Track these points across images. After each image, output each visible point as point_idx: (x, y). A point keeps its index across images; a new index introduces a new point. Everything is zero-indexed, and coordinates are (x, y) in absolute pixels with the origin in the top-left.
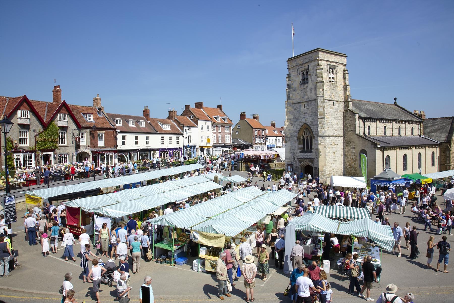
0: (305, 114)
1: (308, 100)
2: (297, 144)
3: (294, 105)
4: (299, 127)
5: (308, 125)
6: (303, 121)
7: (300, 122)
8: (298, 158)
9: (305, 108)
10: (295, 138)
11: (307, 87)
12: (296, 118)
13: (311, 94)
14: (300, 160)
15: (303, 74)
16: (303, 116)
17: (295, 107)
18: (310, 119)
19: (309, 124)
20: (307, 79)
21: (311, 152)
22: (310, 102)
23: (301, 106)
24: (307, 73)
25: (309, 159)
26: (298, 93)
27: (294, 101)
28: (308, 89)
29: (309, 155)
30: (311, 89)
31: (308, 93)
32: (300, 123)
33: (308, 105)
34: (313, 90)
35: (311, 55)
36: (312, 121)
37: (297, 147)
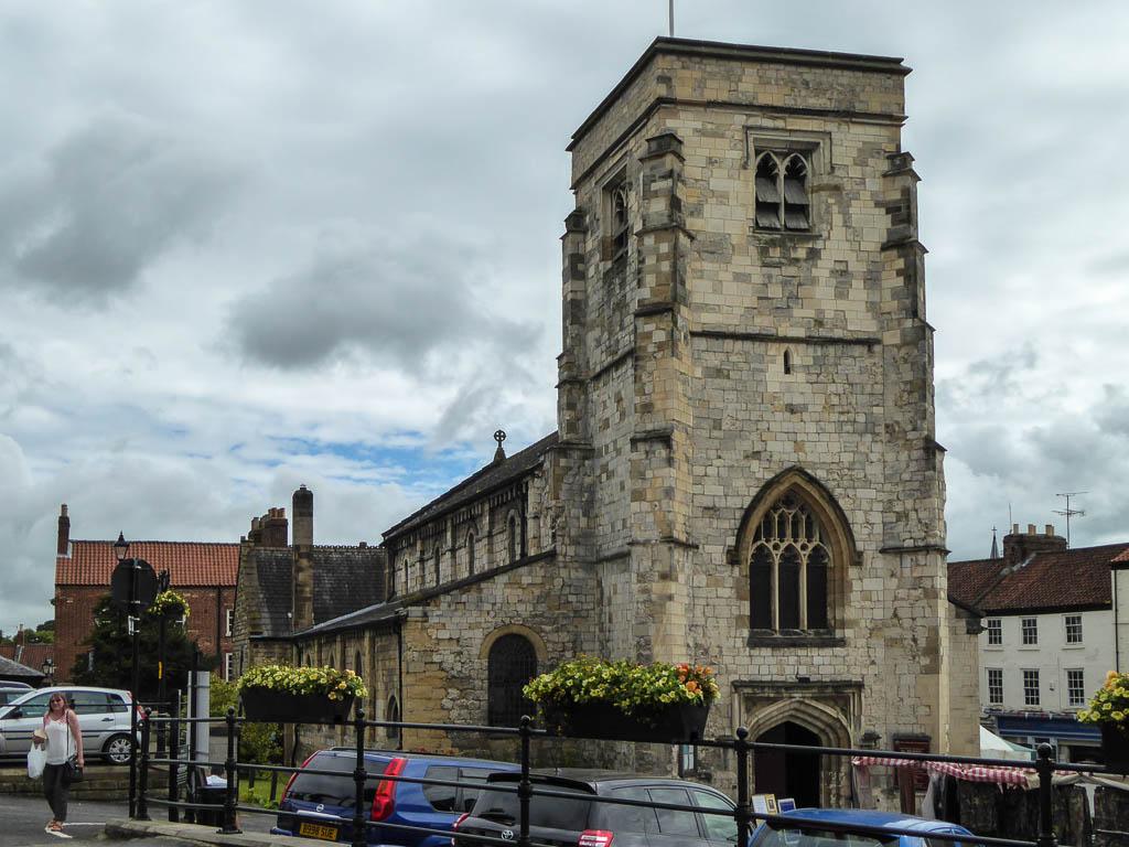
0: (792, 409)
1: (823, 333)
2: (726, 592)
3: (702, 343)
4: (745, 492)
5: (812, 480)
6: (782, 453)
7: (756, 455)
8: (737, 686)
9: (799, 377)
10: (716, 552)
11: (814, 255)
12: (717, 425)
13: (842, 304)
14: (753, 693)
15: (765, 172)
16: (780, 422)
17: (714, 360)
18: (835, 447)
19: (820, 474)
20: (800, 210)
21: (842, 643)
22: (831, 350)
23: (761, 358)
24: (796, 174)
25: (822, 685)
26: (740, 277)
27: (710, 320)
28: (823, 269)
29: (821, 663)
30: (842, 274)
31: (822, 292)
32: (755, 464)
33: (819, 362)
34: (858, 284)
35: (845, 78)
36: (847, 458)
37: (725, 612)
